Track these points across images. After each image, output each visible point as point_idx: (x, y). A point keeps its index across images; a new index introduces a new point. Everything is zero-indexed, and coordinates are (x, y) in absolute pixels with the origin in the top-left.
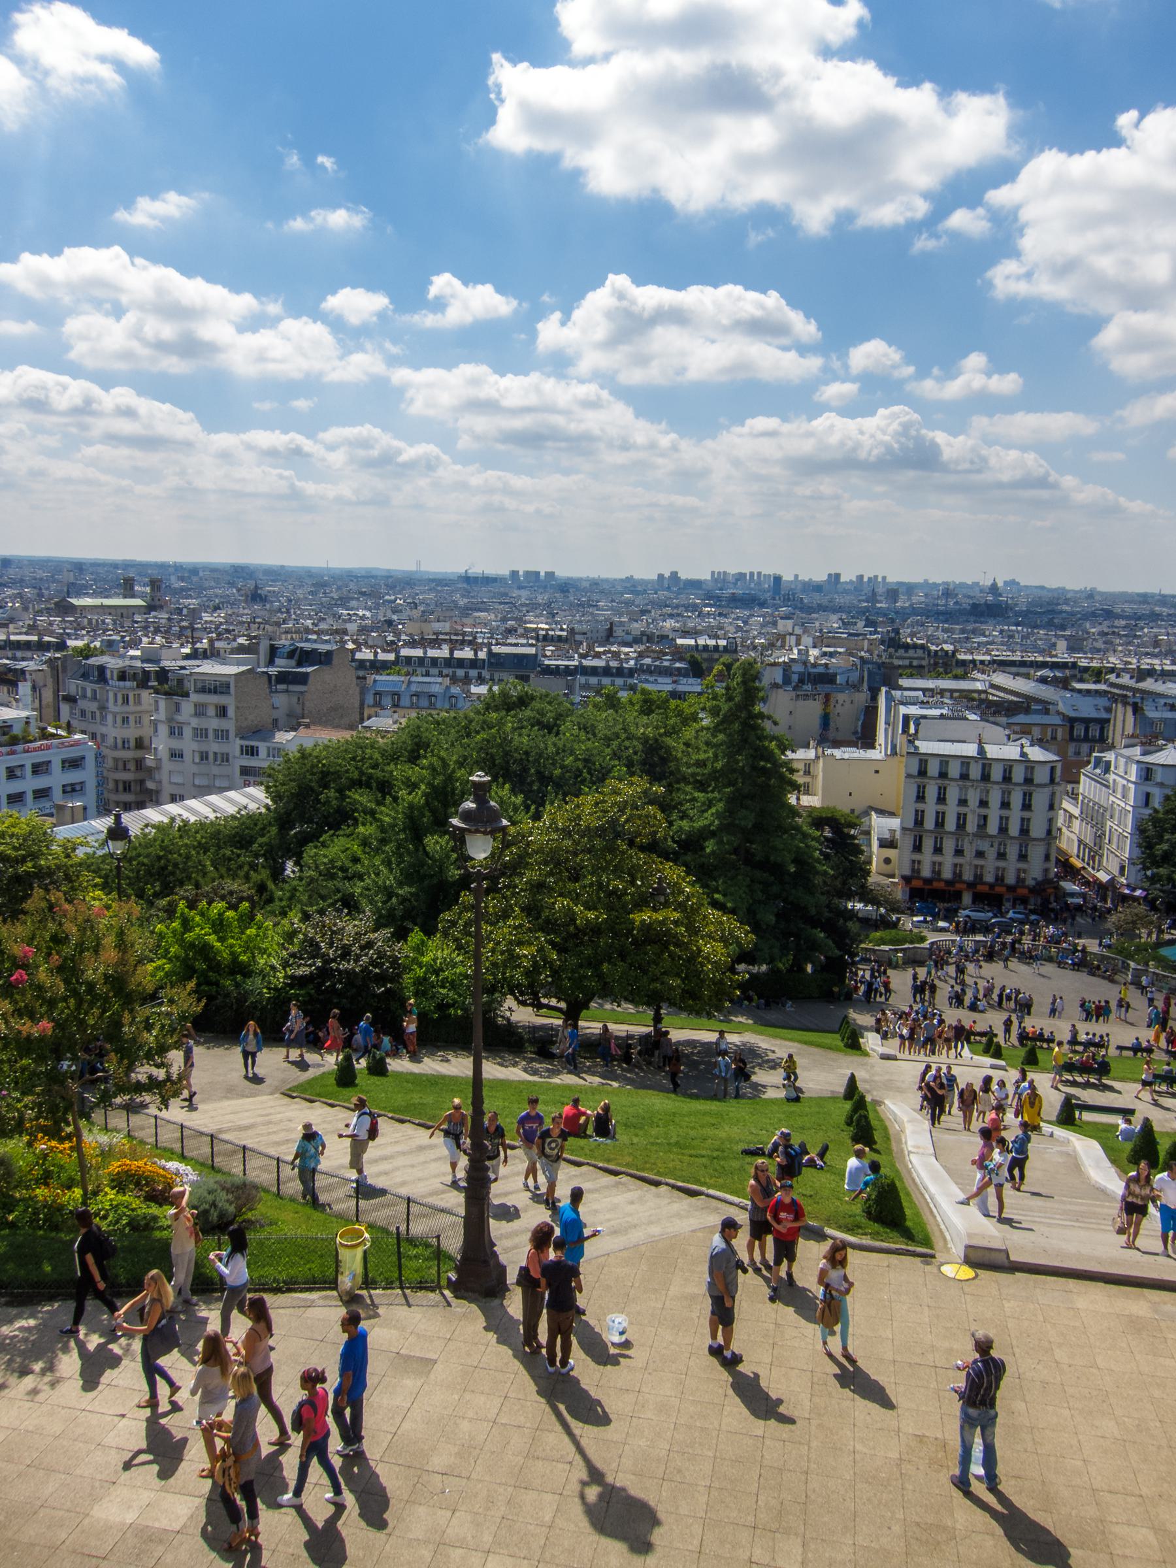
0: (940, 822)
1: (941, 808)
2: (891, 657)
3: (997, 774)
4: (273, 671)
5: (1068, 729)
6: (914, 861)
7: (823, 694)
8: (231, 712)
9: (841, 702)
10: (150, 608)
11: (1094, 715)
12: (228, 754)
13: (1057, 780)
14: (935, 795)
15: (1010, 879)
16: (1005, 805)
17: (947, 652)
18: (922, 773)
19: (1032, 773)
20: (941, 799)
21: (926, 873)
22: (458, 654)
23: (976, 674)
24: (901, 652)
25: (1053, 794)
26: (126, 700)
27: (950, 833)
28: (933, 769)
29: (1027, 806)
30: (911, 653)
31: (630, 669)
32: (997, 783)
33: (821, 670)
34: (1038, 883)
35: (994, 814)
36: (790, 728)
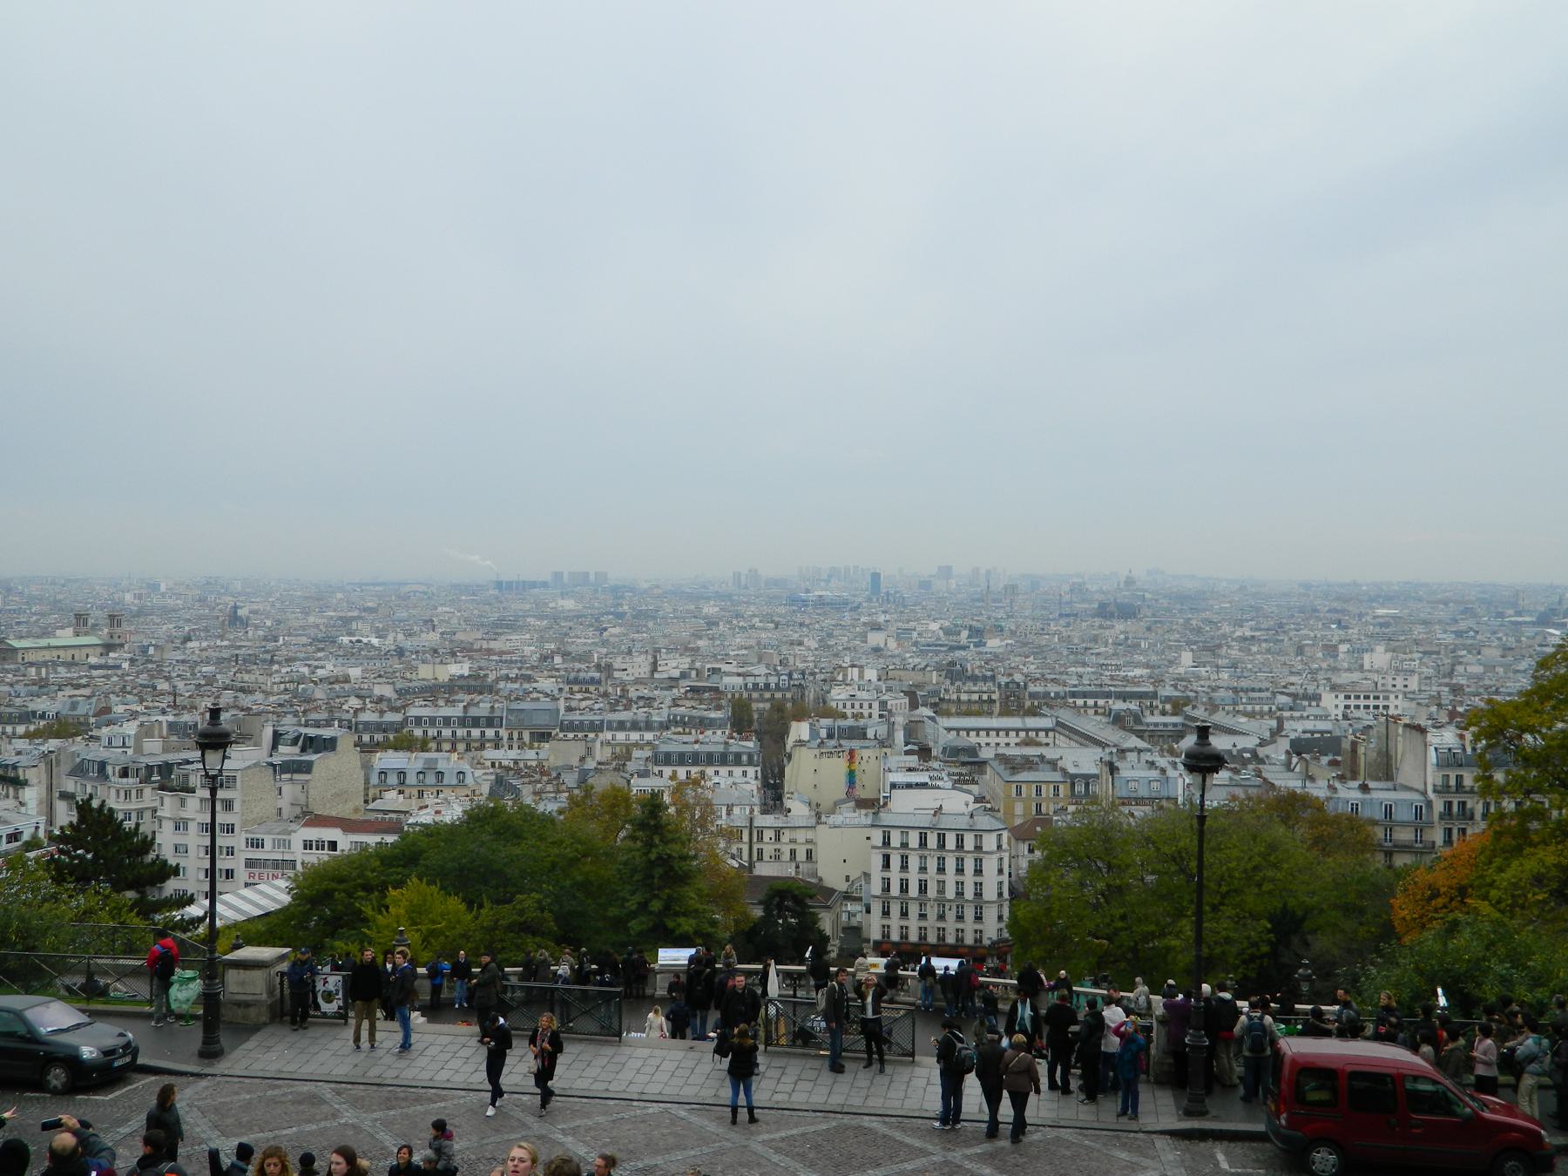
0: (904, 887)
1: (904, 875)
2: (959, 691)
4: (276, 760)
5: (1068, 785)
6: (884, 926)
7: (847, 753)
8: (237, 806)
10: (109, 647)
11: (1094, 771)
12: (232, 848)
13: (1005, 846)
14: (899, 864)
16: (960, 871)
17: (1018, 684)
18: (886, 842)
20: (904, 867)
22: (473, 712)
23: (1045, 710)
24: (970, 686)
25: (1001, 859)
26: (127, 794)
28: (896, 840)
29: (978, 871)
30: (981, 686)
31: (661, 723)
32: (952, 851)
33: (850, 722)
34: (993, 943)
35: (950, 877)
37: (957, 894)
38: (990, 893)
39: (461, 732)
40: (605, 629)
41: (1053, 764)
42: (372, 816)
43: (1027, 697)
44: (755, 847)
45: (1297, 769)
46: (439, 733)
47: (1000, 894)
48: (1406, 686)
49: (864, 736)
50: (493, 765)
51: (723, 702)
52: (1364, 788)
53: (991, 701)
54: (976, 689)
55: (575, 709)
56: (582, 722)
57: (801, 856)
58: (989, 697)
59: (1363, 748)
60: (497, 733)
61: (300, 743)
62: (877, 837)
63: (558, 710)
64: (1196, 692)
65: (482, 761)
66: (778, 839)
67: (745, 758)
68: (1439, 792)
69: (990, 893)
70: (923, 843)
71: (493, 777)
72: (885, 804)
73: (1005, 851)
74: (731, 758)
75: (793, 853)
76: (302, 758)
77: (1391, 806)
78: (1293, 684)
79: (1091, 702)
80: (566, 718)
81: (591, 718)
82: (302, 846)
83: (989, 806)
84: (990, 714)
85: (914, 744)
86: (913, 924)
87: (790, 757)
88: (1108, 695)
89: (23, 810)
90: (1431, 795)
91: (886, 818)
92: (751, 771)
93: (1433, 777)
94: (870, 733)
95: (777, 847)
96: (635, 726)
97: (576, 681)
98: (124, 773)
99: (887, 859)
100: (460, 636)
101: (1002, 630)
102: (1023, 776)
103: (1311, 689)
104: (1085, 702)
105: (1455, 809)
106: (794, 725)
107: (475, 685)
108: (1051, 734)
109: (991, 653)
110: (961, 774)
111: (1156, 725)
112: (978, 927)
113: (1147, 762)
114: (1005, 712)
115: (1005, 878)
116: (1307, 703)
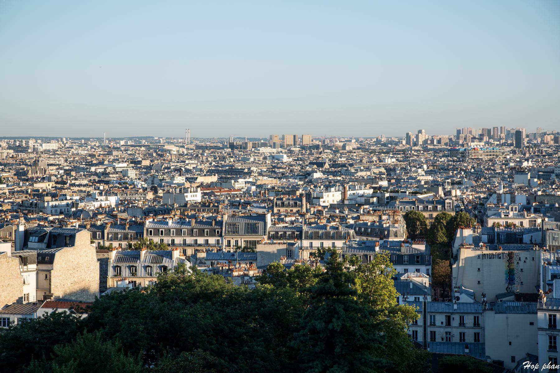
9: (523, 259)
36: (479, 282)
39: (189, 240)
44: (429, 330)
46: (173, 241)
49: (521, 241)
57: (470, 339)
60: (218, 241)
61: (46, 240)
65: (203, 261)
66: (449, 323)
75: (462, 335)
80: (271, 230)
92: (423, 268)
94: (526, 238)
95: (448, 330)
100: (200, 179)
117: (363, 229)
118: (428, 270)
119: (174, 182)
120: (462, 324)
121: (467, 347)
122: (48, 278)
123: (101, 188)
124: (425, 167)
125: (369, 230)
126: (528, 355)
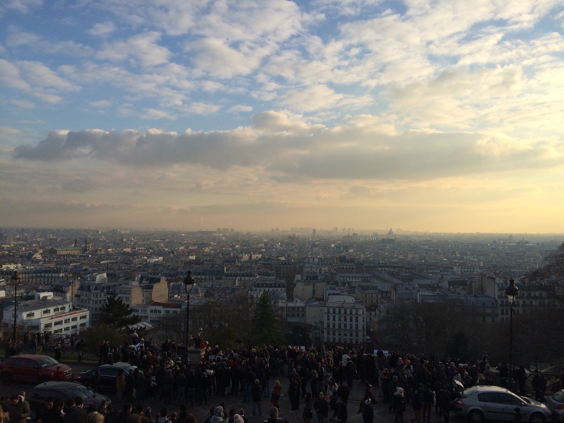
0: (334, 325)
1: (334, 322)
2: (343, 265)
3: (348, 312)
4: (142, 285)
5: (381, 294)
6: (328, 338)
7: (312, 285)
9: (318, 286)
11: (389, 290)
13: (364, 313)
15: (354, 342)
16: (351, 320)
17: (361, 263)
18: (329, 312)
19: (358, 311)
20: (334, 319)
21: (331, 341)
27: (337, 329)
29: (357, 321)
35: (348, 323)
37: (350, 328)
38: (360, 328)
40: (234, 246)
41: (375, 288)
42: (171, 302)
43: (364, 267)
45: (452, 290)
47: (363, 328)
48: (479, 265)
50: (205, 287)
51: (273, 268)
52: (476, 296)
53: (353, 268)
54: (348, 265)
55: (229, 270)
56: (231, 274)
58: (352, 267)
59: (474, 284)
61: (149, 280)
62: (326, 310)
63: (224, 270)
64: (415, 266)
65: (202, 286)
67: (281, 285)
68: (499, 298)
69: (360, 328)
70: (340, 312)
71: (205, 291)
72: (328, 300)
73: (365, 315)
74: (277, 285)
76: (150, 285)
77: (484, 302)
78: (444, 264)
79: (383, 269)
80: (227, 273)
81: (234, 273)
82: (150, 311)
83: (359, 301)
84: (353, 272)
85: (333, 281)
86: (337, 337)
87: (295, 286)
88: (388, 267)
89: (65, 300)
90: (496, 298)
91: (327, 304)
92: (283, 289)
93: (497, 293)
94: (319, 278)
96: (247, 276)
97: (228, 261)
98: (96, 289)
99: (328, 316)
100: (190, 248)
101: (353, 247)
102: (367, 292)
103: (450, 265)
104: (382, 269)
105: (505, 303)
106: (296, 275)
107: (197, 262)
108: (372, 279)
109: (350, 254)
110: (349, 291)
111: (404, 276)
112: (357, 338)
113: (406, 288)
114: (357, 272)
115: (365, 323)
116: (449, 270)
117: (260, 273)
118: (285, 289)
119: (180, 248)
120: (298, 310)
121: (300, 319)
122: (151, 294)
123: (151, 251)
124: (279, 243)
125: (262, 273)
126: (320, 321)
